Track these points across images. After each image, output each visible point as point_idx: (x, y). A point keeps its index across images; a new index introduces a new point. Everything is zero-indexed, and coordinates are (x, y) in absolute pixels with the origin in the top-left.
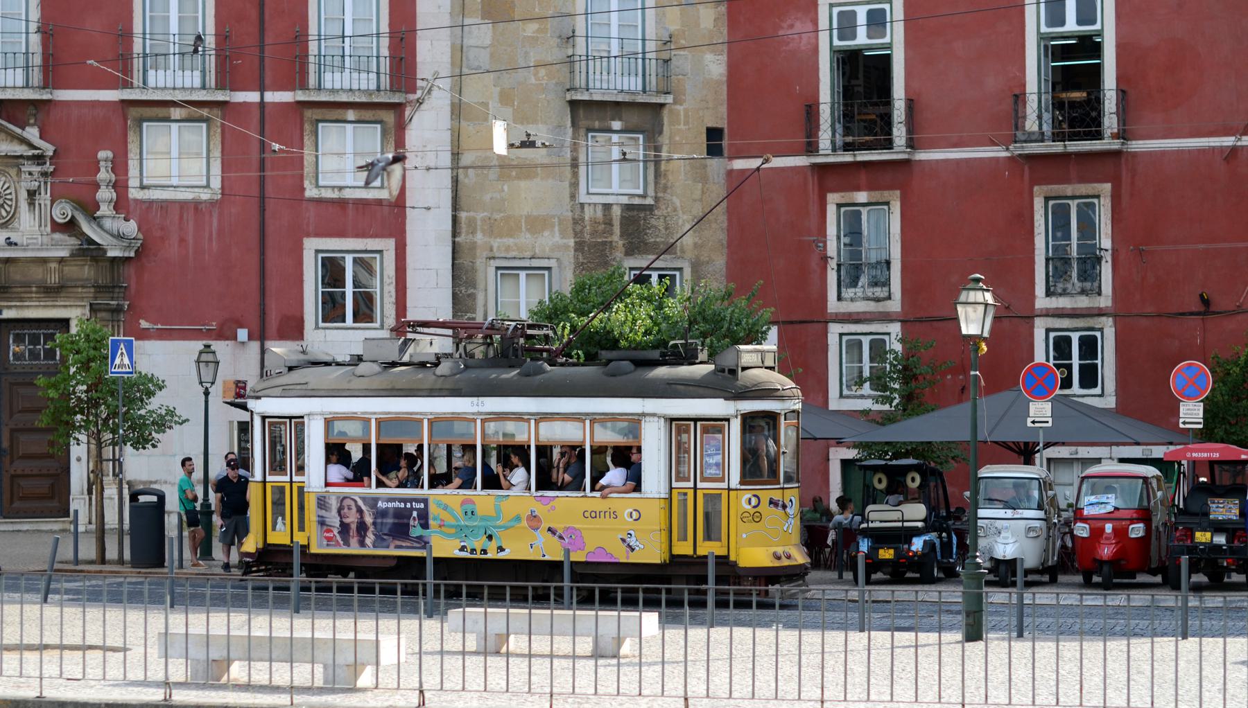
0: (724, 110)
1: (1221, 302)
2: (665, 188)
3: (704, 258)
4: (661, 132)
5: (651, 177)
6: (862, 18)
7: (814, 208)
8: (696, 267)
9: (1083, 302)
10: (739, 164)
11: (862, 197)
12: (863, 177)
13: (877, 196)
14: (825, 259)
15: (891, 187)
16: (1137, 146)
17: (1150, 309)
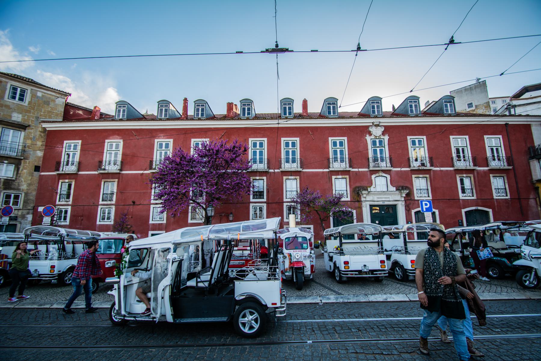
0: (41, 163)
1: (137, 203)
2: (20, 177)
3: (30, 192)
4: (20, 165)
5: (15, 174)
6: (73, 145)
7: (56, 183)
8: (26, 194)
9: (109, 203)
10: (42, 174)
11: (67, 181)
12: (68, 177)
13: (70, 180)
14: (57, 193)
15: (73, 179)
16: (124, 172)
17: (123, 204)
